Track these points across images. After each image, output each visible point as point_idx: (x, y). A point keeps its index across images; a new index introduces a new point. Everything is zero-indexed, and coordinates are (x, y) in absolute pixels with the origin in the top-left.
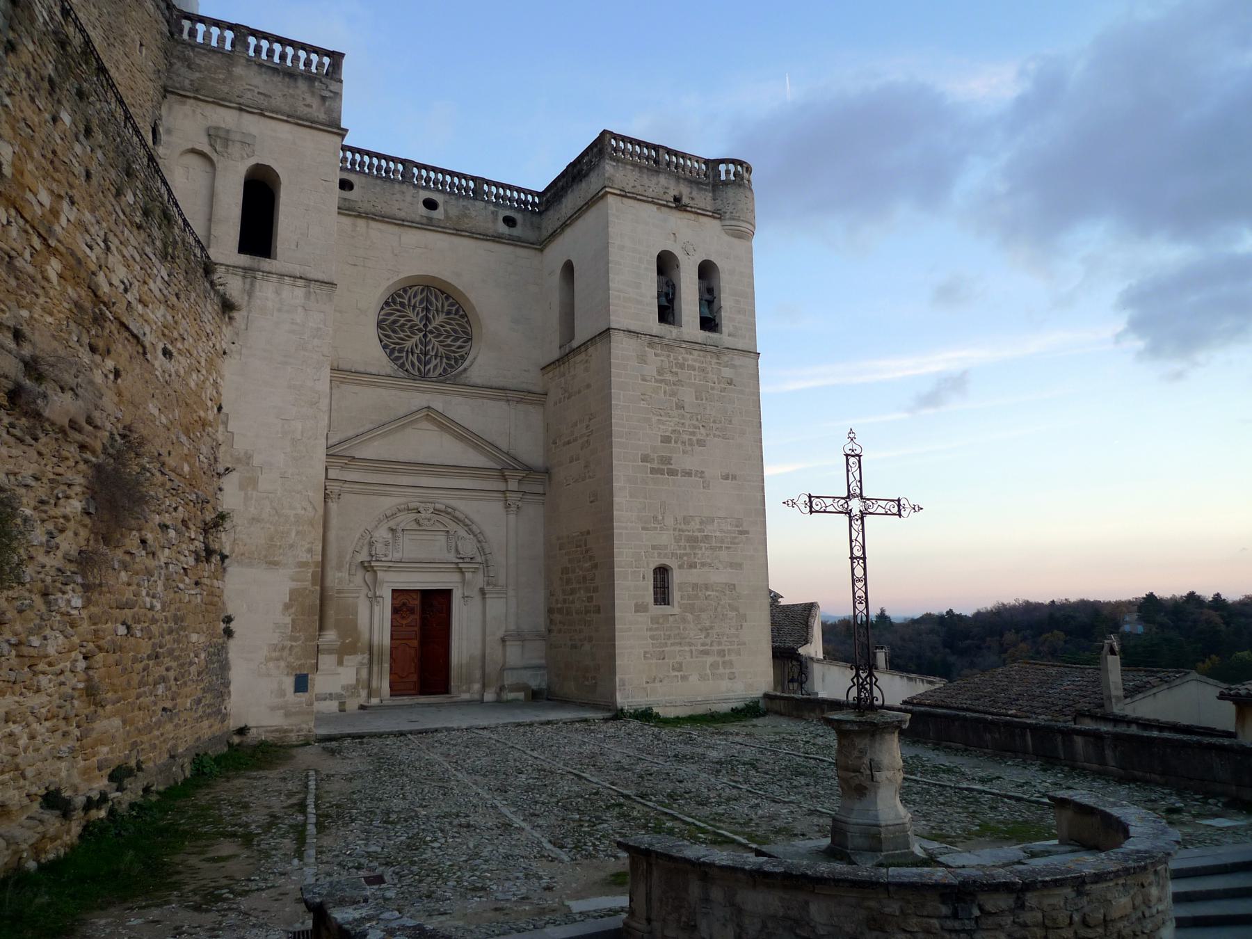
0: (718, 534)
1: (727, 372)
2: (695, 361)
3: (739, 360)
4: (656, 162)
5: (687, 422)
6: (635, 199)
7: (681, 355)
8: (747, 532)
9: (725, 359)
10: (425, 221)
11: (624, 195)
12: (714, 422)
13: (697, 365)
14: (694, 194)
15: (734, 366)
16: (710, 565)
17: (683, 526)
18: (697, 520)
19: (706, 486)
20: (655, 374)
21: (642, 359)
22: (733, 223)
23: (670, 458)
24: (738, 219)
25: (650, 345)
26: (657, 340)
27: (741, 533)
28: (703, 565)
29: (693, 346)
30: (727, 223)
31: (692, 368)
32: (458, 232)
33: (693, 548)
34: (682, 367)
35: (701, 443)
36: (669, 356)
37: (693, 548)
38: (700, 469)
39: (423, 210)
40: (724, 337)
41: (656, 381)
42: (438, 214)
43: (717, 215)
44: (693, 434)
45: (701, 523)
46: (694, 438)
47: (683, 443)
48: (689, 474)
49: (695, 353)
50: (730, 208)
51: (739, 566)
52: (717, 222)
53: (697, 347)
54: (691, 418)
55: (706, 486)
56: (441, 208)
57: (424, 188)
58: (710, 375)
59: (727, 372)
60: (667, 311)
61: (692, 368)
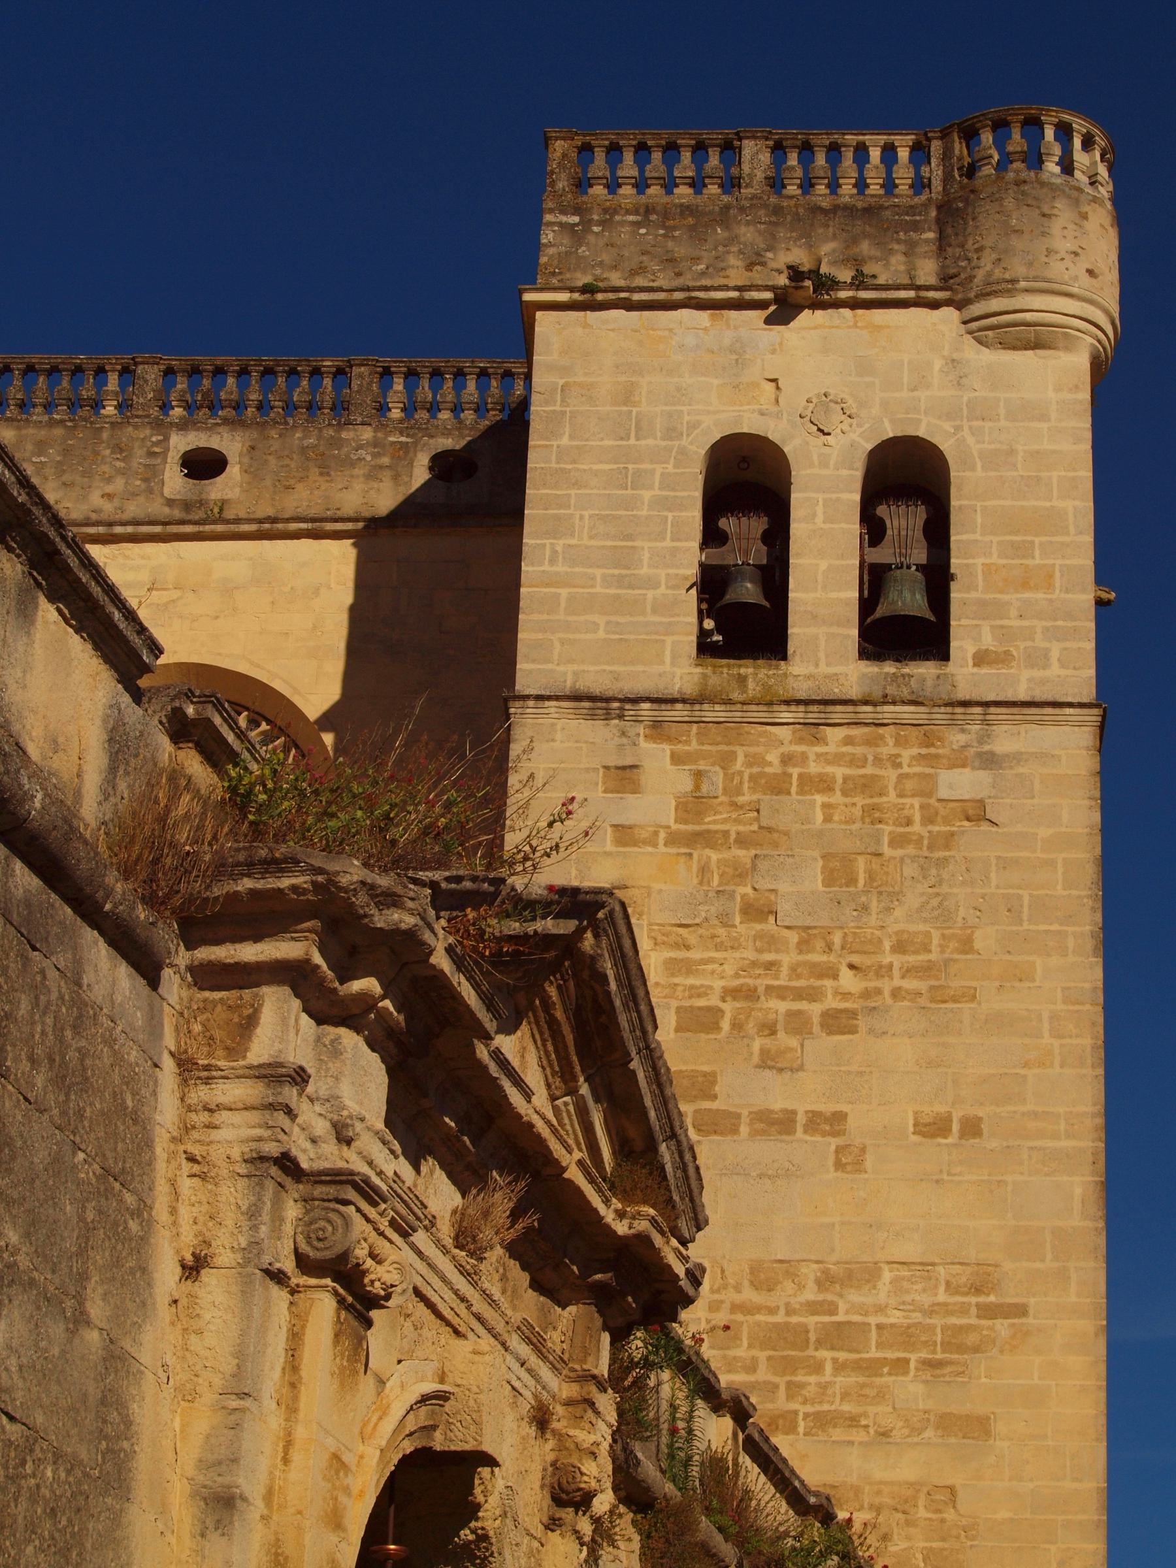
0: (895, 1317)
1: (960, 783)
2: (837, 759)
3: (1009, 738)
4: (731, 184)
5: (787, 959)
6: (629, 306)
7: (779, 741)
8: (1021, 1311)
9: (957, 738)
10: (177, 514)
11: (590, 300)
12: (900, 947)
13: (839, 772)
14: (865, 247)
15: (990, 761)
16: (853, 1421)
17: (756, 1297)
18: (810, 1272)
19: (849, 1160)
20: (669, 817)
21: (625, 777)
22: (995, 304)
23: (711, 1079)
24: (1009, 287)
25: (657, 729)
26: (679, 712)
27: (989, 1312)
28: (822, 1421)
29: (814, 714)
30: (977, 309)
31: (824, 784)
32: (270, 529)
33: (788, 1366)
34: (778, 786)
35: (838, 1022)
36: (726, 760)
37: (788, 1366)
38: (827, 1108)
39: (174, 481)
40: (963, 671)
41: (673, 839)
42: (225, 488)
43: (953, 290)
44: (812, 995)
45: (826, 1281)
46: (815, 1010)
47: (770, 1029)
48: (779, 1124)
49: (834, 735)
50: (987, 259)
51: (977, 1427)
52: (949, 314)
53: (838, 713)
54: (804, 945)
55: (849, 1160)
56: (233, 471)
57: (183, 426)
58: (892, 797)
59: (960, 783)
60: (744, 620)
61: (824, 784)
